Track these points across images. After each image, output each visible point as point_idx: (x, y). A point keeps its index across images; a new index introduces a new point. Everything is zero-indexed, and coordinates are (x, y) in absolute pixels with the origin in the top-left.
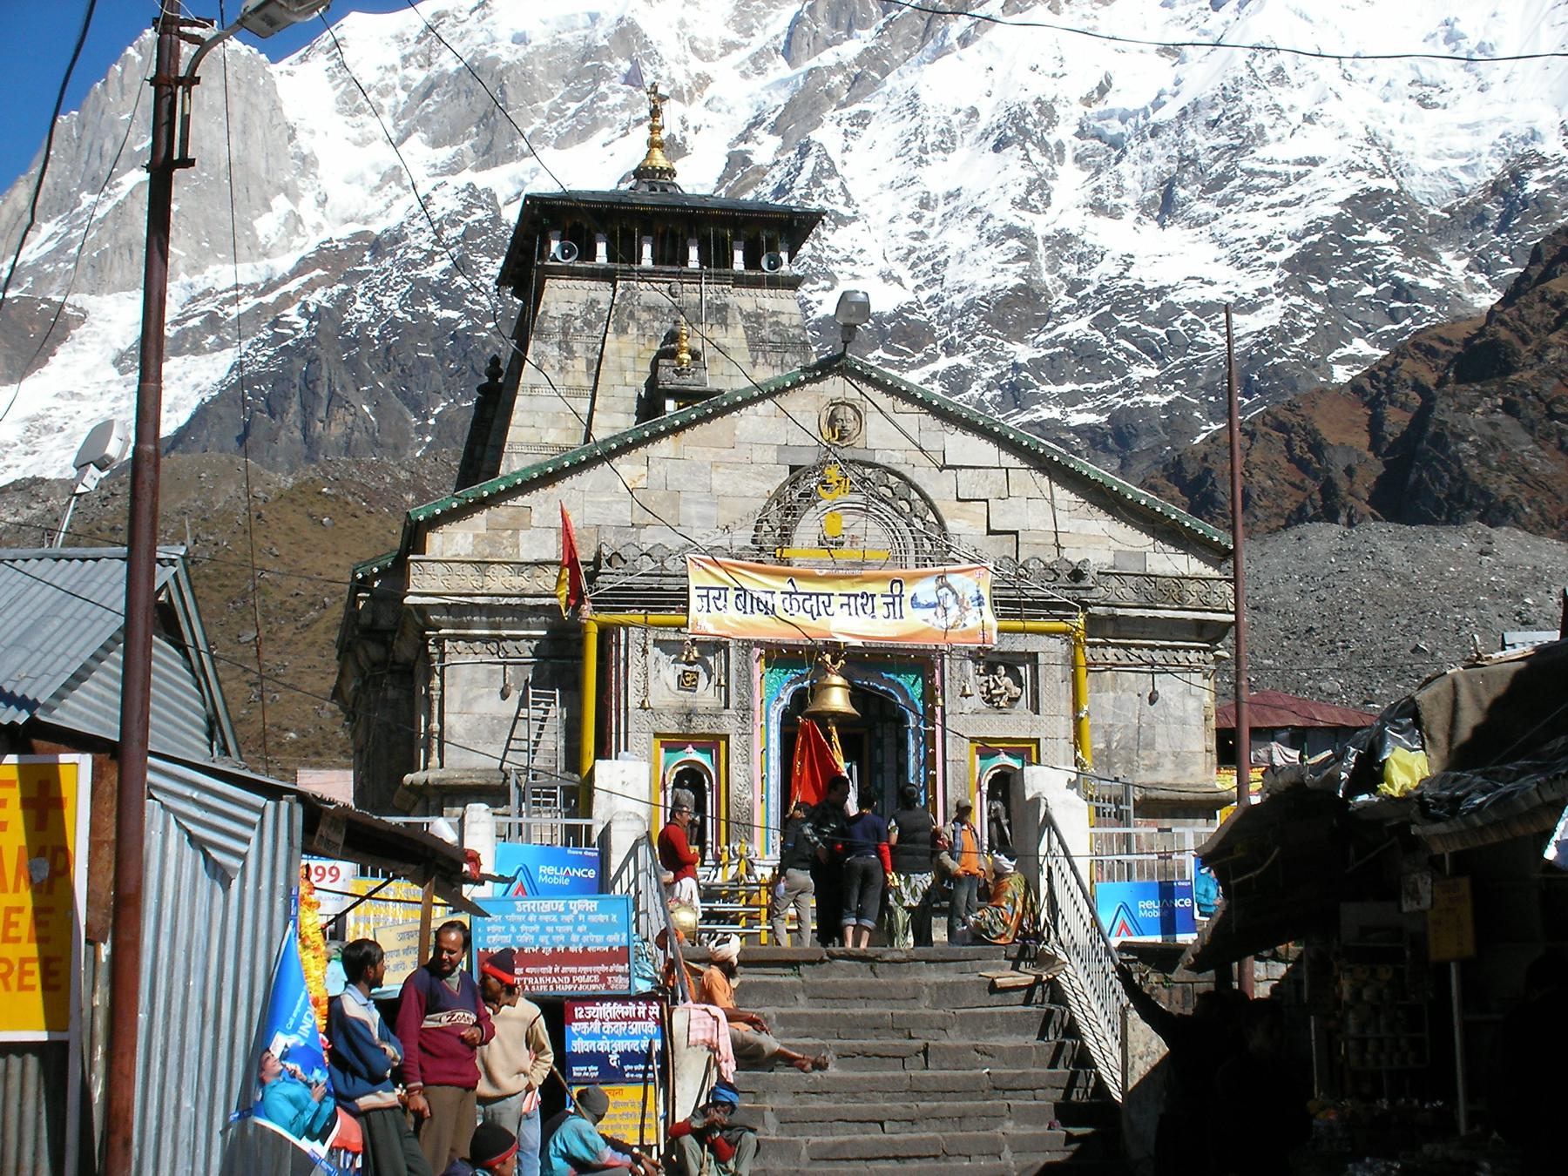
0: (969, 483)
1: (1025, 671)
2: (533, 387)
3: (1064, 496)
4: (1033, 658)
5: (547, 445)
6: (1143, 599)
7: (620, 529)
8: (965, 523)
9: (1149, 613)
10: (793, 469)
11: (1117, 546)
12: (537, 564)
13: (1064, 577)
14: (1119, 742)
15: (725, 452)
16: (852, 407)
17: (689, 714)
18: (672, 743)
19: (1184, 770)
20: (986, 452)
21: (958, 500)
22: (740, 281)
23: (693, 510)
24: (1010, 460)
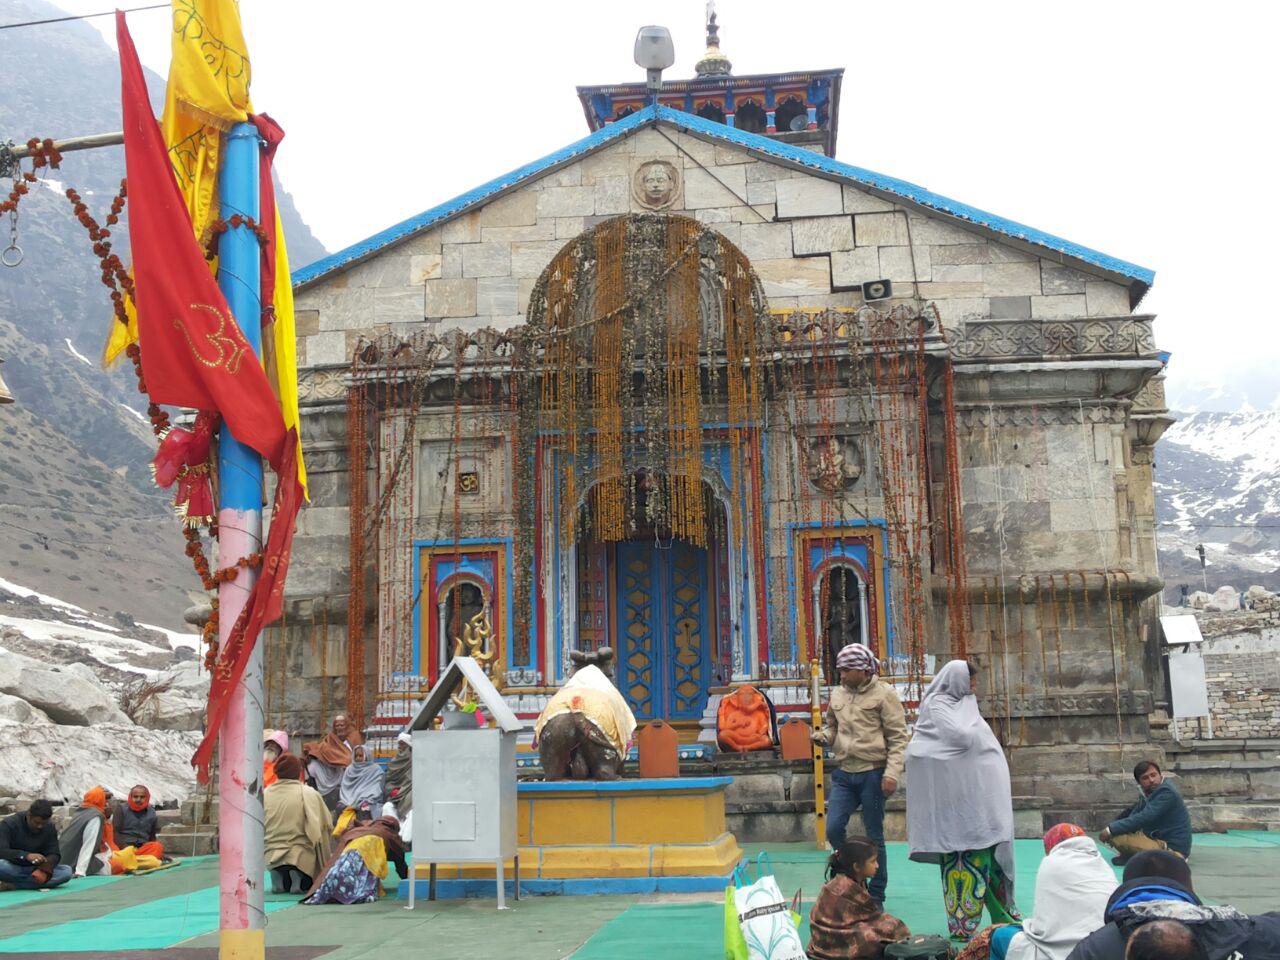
0: (806, 237)
6: (1024, 351)
8: (803, 283)
9: (1032, 366)
15: (526, 231)
16: (656, 162)
17: (459, 521)
18: (440, 558)
19: (1091, 552)
21: (795, 256)
24: (856, 203)
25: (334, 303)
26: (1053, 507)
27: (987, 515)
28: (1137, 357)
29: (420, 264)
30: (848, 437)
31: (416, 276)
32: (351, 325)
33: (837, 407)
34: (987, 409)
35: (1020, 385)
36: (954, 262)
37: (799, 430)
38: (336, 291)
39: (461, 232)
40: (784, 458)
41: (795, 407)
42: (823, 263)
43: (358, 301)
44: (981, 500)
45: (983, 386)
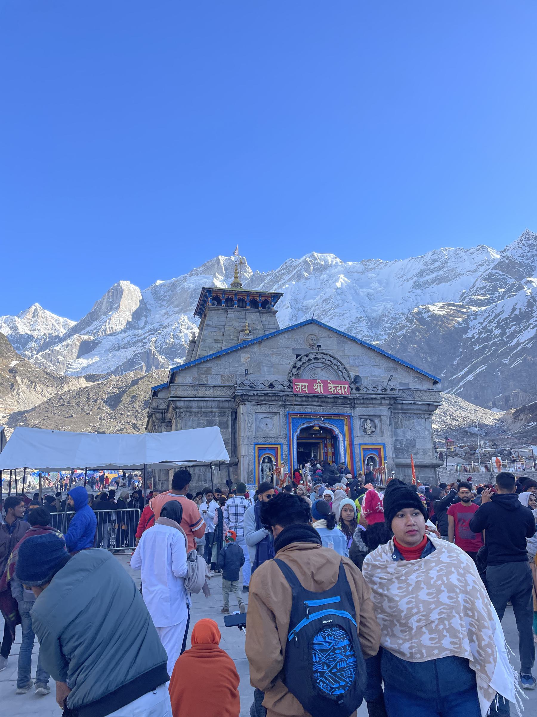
1: (377, 421)
4: (380, 416)
10: (297, 356)
13: (389, 390)
14: (405, 445)
15: (275, 350)
25: (217, 366)
26: (417, 441)
27: (401, 442)
30: (372, 418)
31: (242, 360)
33: (371, 411)
34: (398, 413)
35: (409, 407)
37: (360, 417)
38: (218, 362)
39: (256, 349)
40: (357, 424)
41: (359, 410)
43: (225, 366)
44: (399, 438)
45: (400, 406)
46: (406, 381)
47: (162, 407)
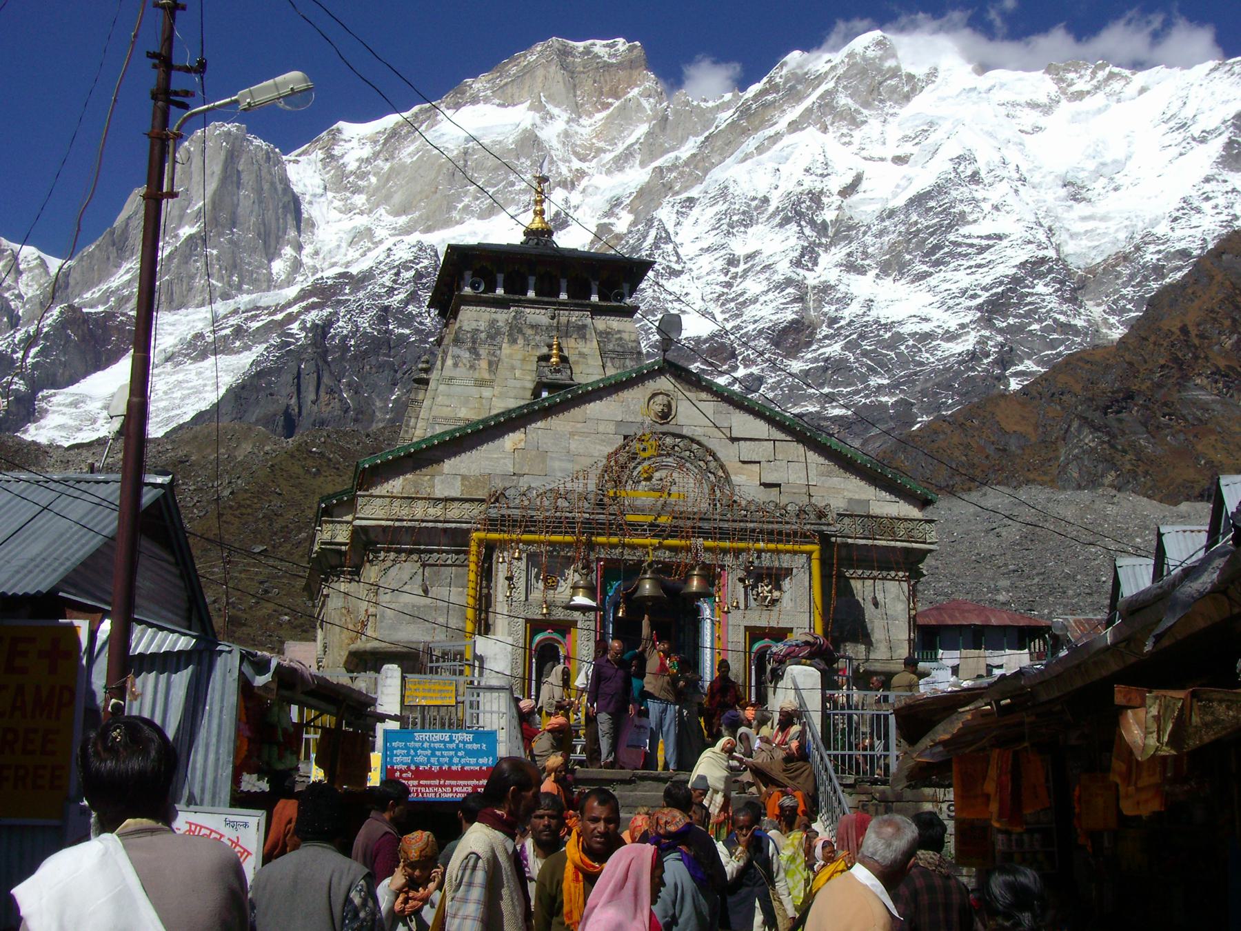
0: (747, 451)
2: (451, 379)
3: (813, 457)
5: (460, 419)
7: (504, 476)
8: (744, 477)
9: (870, 542)
10: (626, 437)
11: (850, 495)
12: (447, 500)
15: (579, 425)
18: (535, 626)
20: (760, 428)
22: (597, 311)
23: (557, 464)
28: (924, 543)
29: (512, 440)
32: (464, 471)
36: (829, 474)
42: (756, 467)
46: (864, 497)
47: (339, 539)
